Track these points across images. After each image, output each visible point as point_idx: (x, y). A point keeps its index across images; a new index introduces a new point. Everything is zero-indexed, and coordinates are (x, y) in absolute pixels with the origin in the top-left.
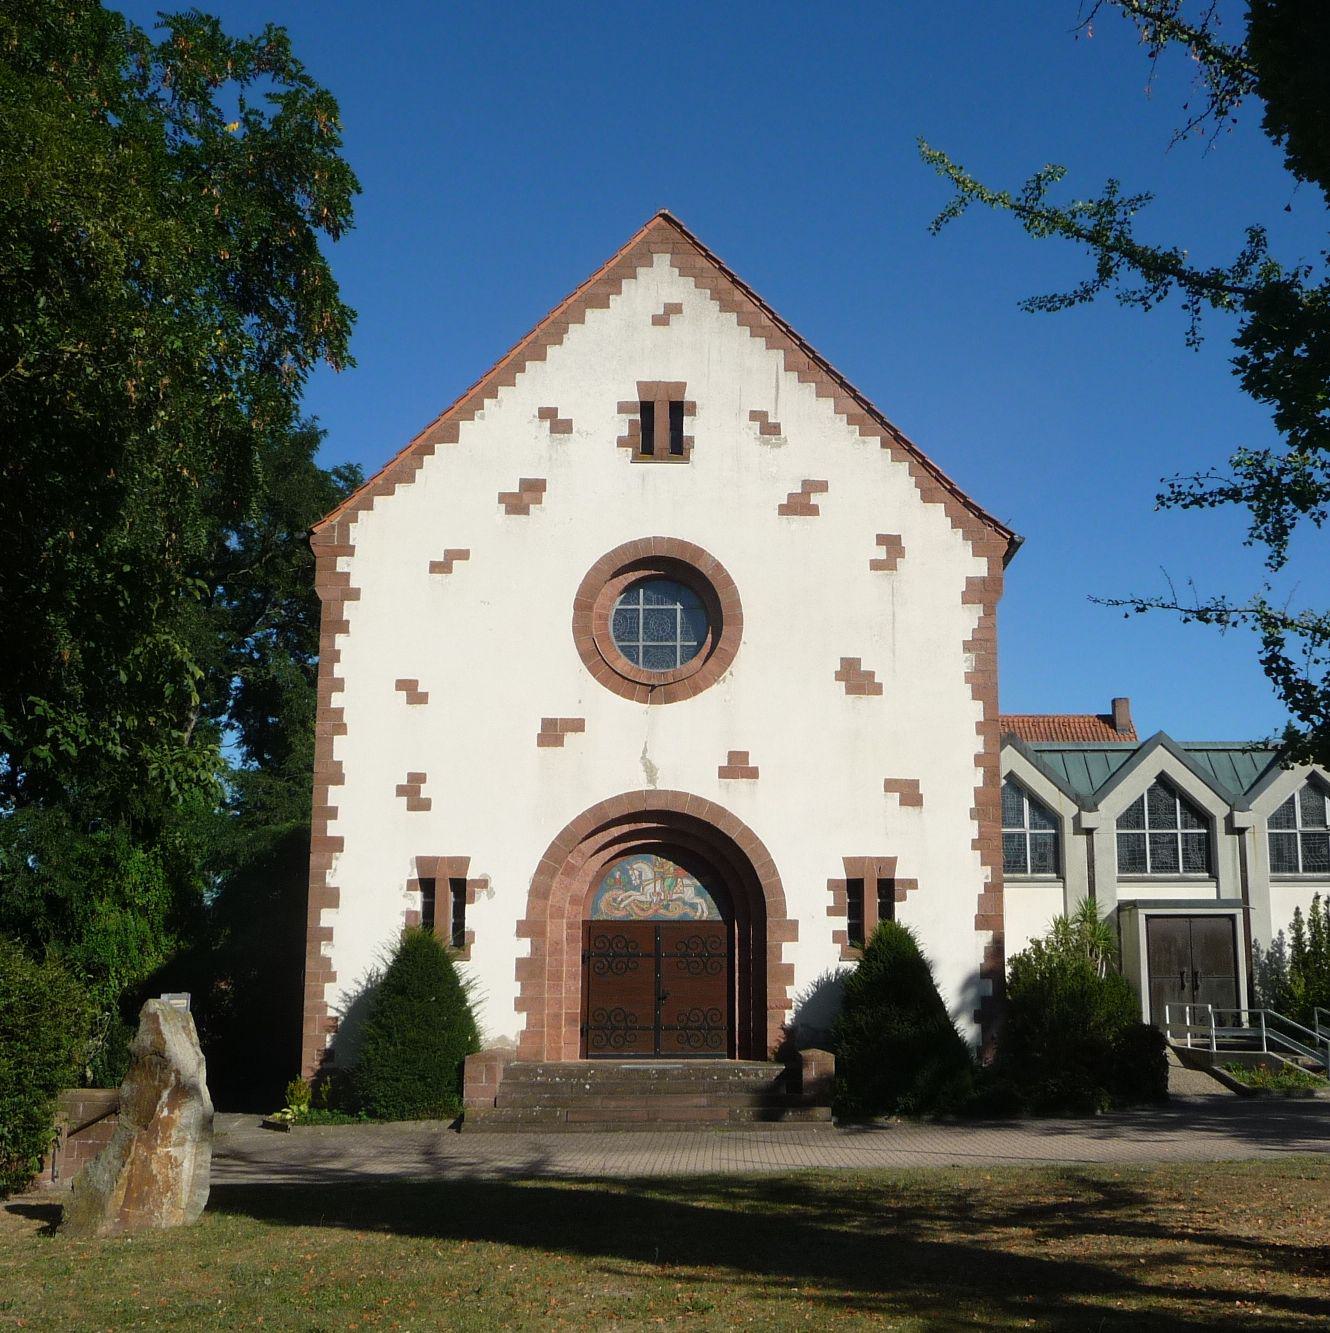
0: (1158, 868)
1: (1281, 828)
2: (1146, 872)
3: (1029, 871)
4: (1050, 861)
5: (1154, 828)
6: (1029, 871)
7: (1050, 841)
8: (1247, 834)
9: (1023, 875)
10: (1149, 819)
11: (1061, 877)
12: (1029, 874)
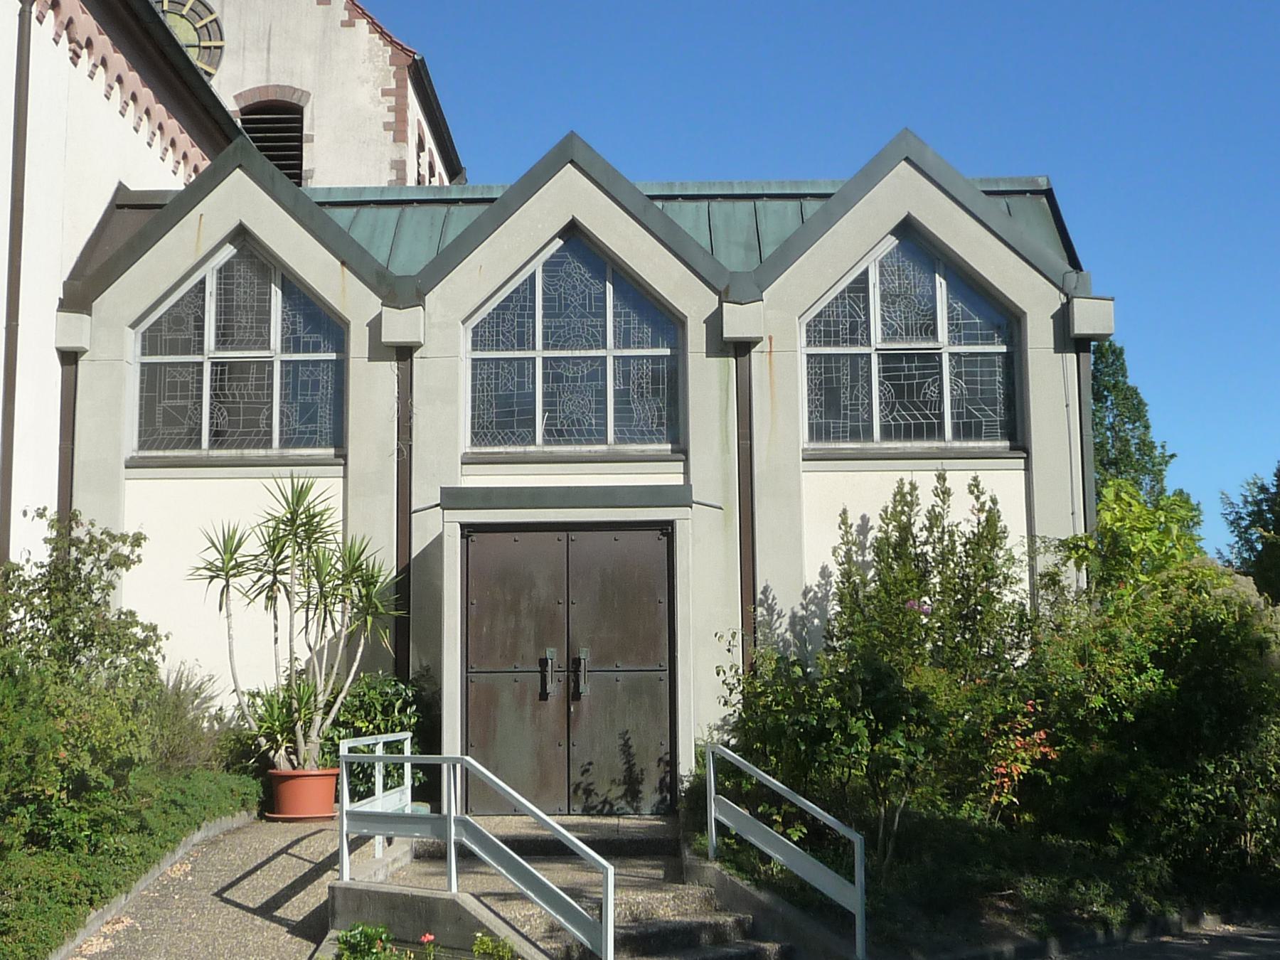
0: (560, 433)
1: (836, 344)
2: (533, 442)
3: (276, 442)
4: (325, 424)
5: (555, 347)
6: (276, 442)
7: (326, 378)
8: (754, 354)
9: (261, 452)
10: (545, 327)
11: (342, 456)
12: (275, 450)
